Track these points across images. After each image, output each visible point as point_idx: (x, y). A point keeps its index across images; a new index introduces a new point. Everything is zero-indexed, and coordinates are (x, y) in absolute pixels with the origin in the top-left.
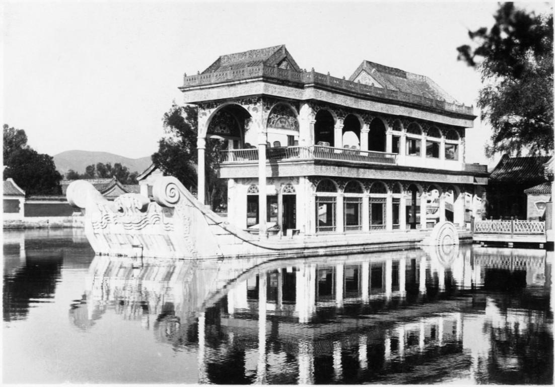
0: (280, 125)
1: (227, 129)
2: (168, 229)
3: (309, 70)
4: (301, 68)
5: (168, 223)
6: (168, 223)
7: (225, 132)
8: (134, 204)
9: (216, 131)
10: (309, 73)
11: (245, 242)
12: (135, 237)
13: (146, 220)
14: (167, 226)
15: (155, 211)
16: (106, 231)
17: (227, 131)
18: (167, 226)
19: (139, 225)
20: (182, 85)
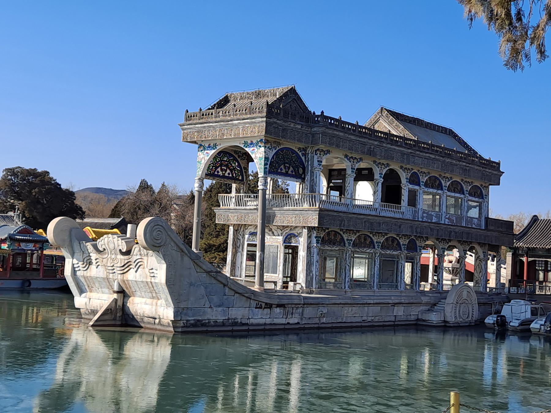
0: (284, 171)
1: (228, 171)
2: (152, 275)
3: (318, 113)
4: (311, 109)
5: (152, 269)
6: (152, 269)
7: (226, 175)
8: (118, 246)
9: (216, 173)
10: (318, 116)
11: (237, 295)
12: (116, 281)
13: (129, 264)
14: (151, 271)
15: (141, 255)
16: (88, 274)
17: (229, 174)
18: (151, 271)
19: (123, 268)
20: (183, 122)
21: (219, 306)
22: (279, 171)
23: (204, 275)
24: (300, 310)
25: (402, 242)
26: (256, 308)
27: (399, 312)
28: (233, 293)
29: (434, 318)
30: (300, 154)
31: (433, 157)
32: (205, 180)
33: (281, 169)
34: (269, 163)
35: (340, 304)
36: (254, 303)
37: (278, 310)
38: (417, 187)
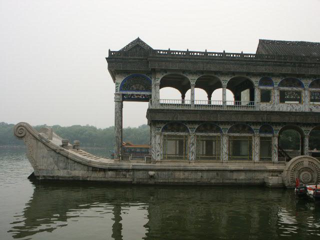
0: (135, 88)
17: (142, 97)
21: (65, 169)
22: (131, 89)
23: (53, 152)
24: (132, 173)
25: (253, 127)
26: (92, 171)
27: (242, 176)
28: (72, 162)
29: (273, 180)
30: (149, 77)
31: (278, 63)
32: (124, 102)
33: (133, 88)
34: (119, 86)
35: (169, 170)
36: (91, 169)
37: (110, 173)
38: (269, 88)
